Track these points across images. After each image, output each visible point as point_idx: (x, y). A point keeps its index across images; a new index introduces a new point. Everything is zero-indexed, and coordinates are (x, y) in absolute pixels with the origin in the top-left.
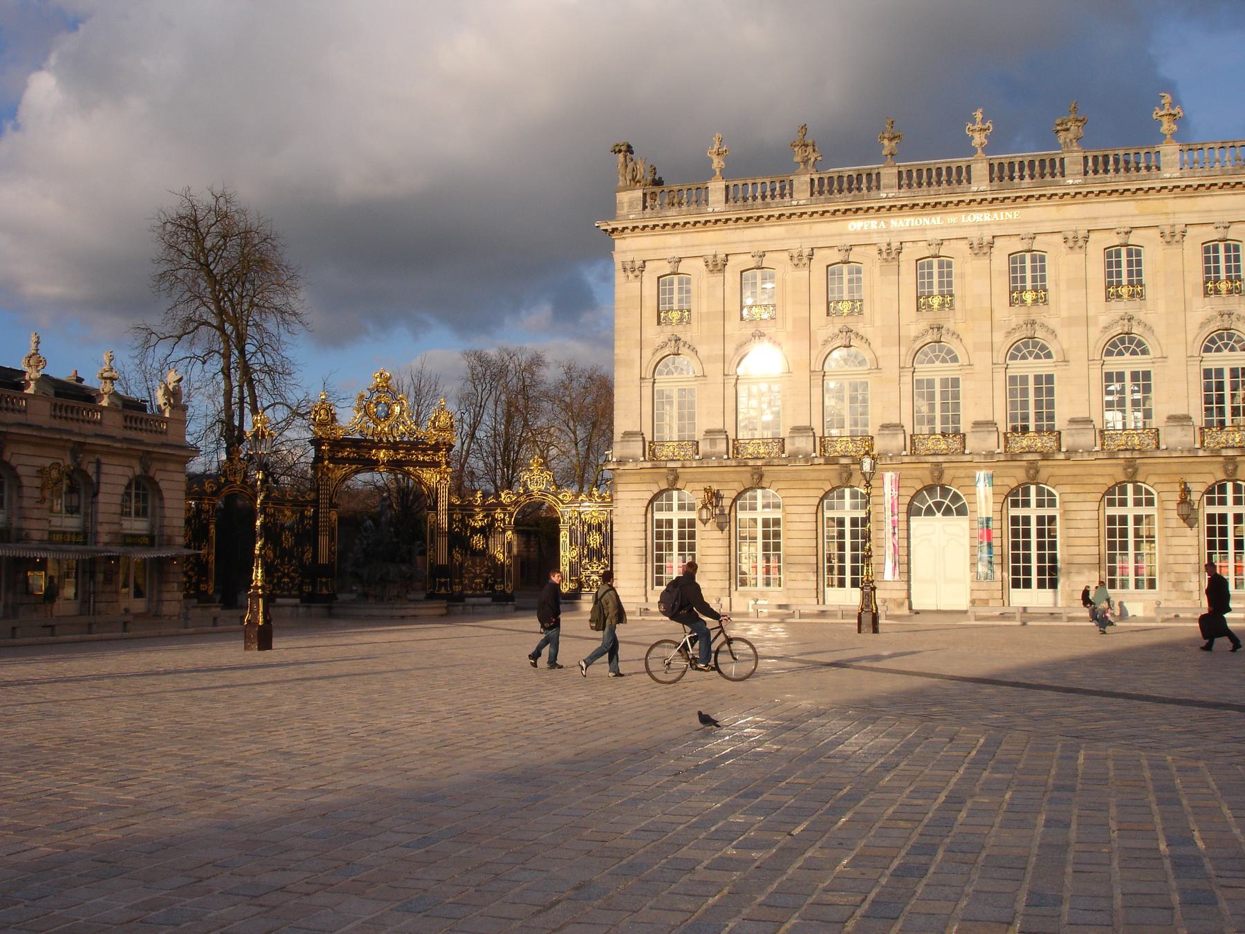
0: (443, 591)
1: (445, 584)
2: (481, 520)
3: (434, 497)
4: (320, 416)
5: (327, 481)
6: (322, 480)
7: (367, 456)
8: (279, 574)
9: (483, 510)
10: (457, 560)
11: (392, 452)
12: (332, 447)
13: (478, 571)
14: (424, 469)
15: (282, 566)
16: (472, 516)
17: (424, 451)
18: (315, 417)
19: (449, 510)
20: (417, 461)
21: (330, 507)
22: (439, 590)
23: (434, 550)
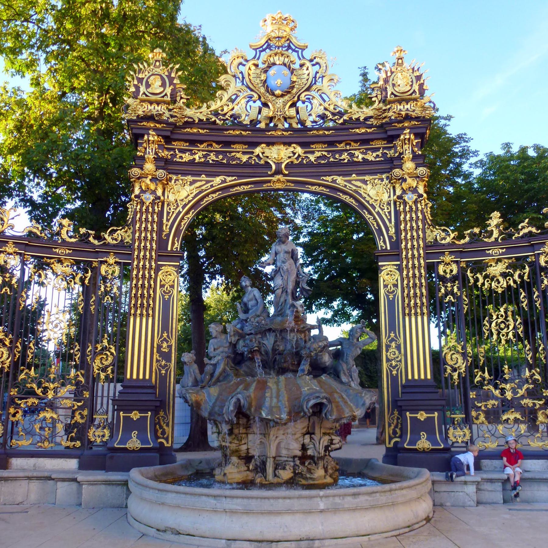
0: (424, 443)
1: (428, 426)
2: (504, 275)
3: (392, 231)
4: (148, 86)
5: (153, 203)
6: (142, 203)
7: (245, 158)
8: (32, 401)
9: (509, 250)
10: (454, 370)
11: (299, 150)
12: (168, 140)
13: (509, 395)
14: (367, 178)
15: (39, 385)
16: (479, 267)
17: (364, 141)
18: (137, 88)
19: (427, 256)
20: (352, 163)
21: (160, 257)
22: (413, 442)
23: (398, 347)
